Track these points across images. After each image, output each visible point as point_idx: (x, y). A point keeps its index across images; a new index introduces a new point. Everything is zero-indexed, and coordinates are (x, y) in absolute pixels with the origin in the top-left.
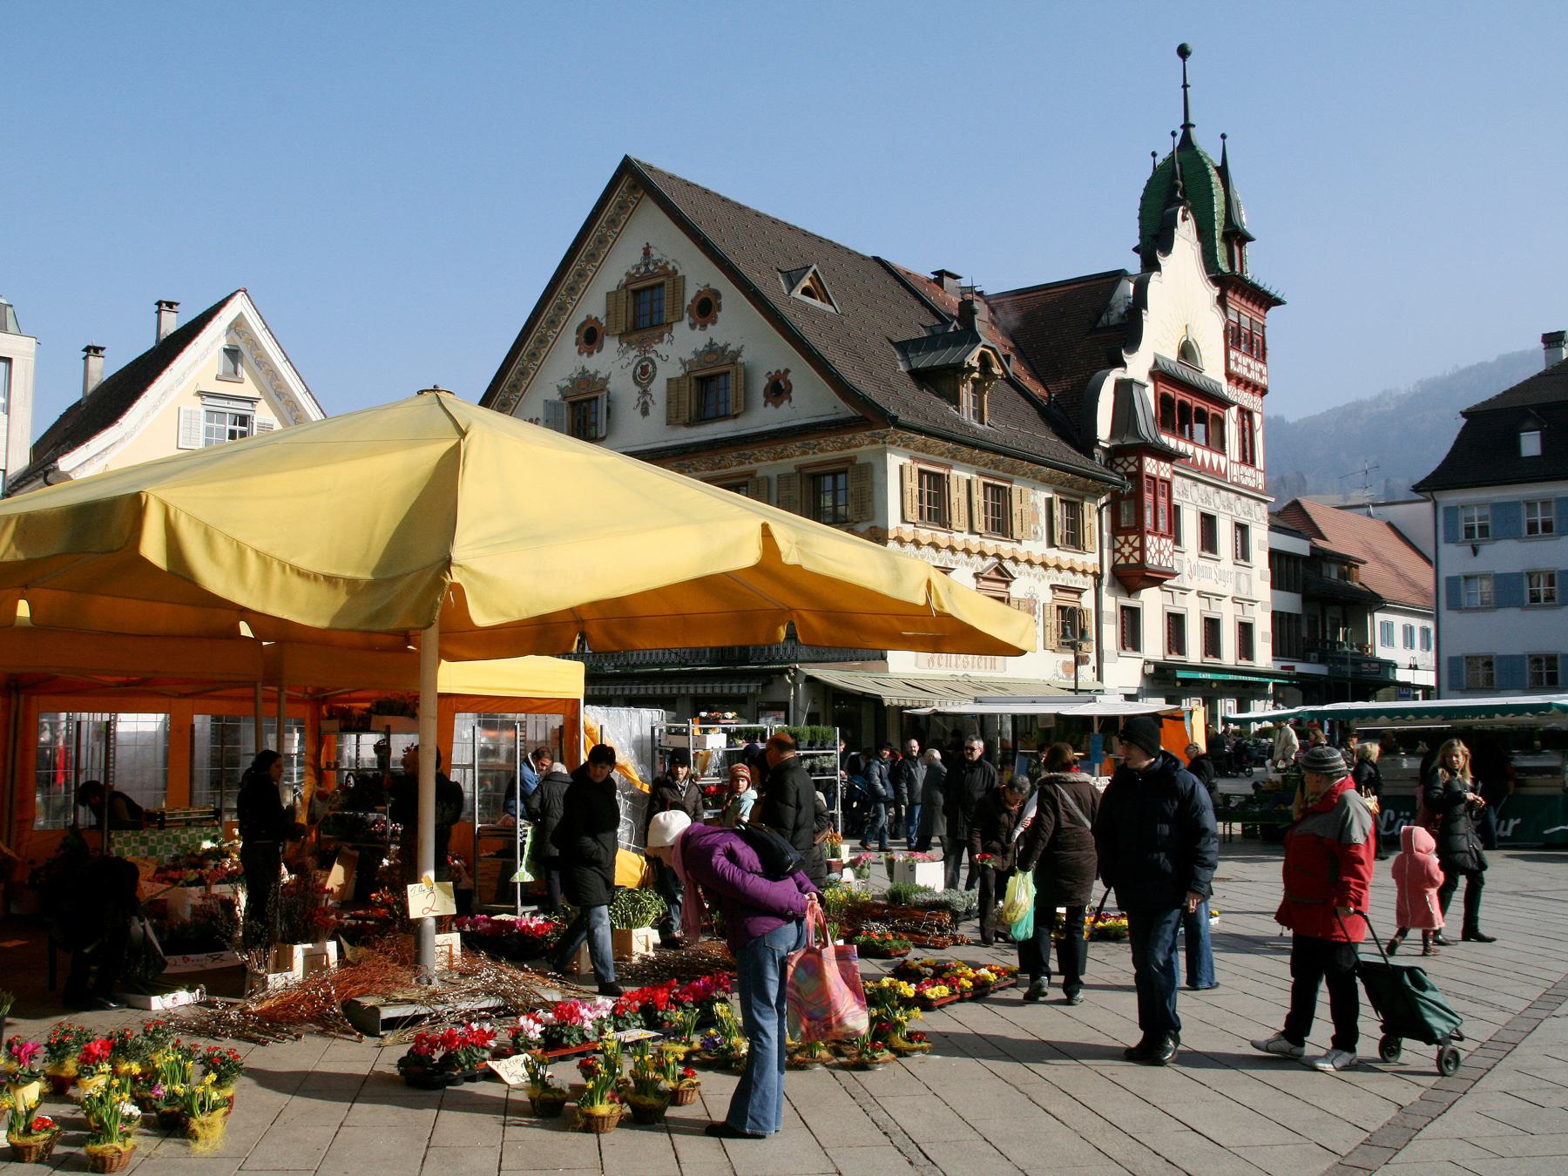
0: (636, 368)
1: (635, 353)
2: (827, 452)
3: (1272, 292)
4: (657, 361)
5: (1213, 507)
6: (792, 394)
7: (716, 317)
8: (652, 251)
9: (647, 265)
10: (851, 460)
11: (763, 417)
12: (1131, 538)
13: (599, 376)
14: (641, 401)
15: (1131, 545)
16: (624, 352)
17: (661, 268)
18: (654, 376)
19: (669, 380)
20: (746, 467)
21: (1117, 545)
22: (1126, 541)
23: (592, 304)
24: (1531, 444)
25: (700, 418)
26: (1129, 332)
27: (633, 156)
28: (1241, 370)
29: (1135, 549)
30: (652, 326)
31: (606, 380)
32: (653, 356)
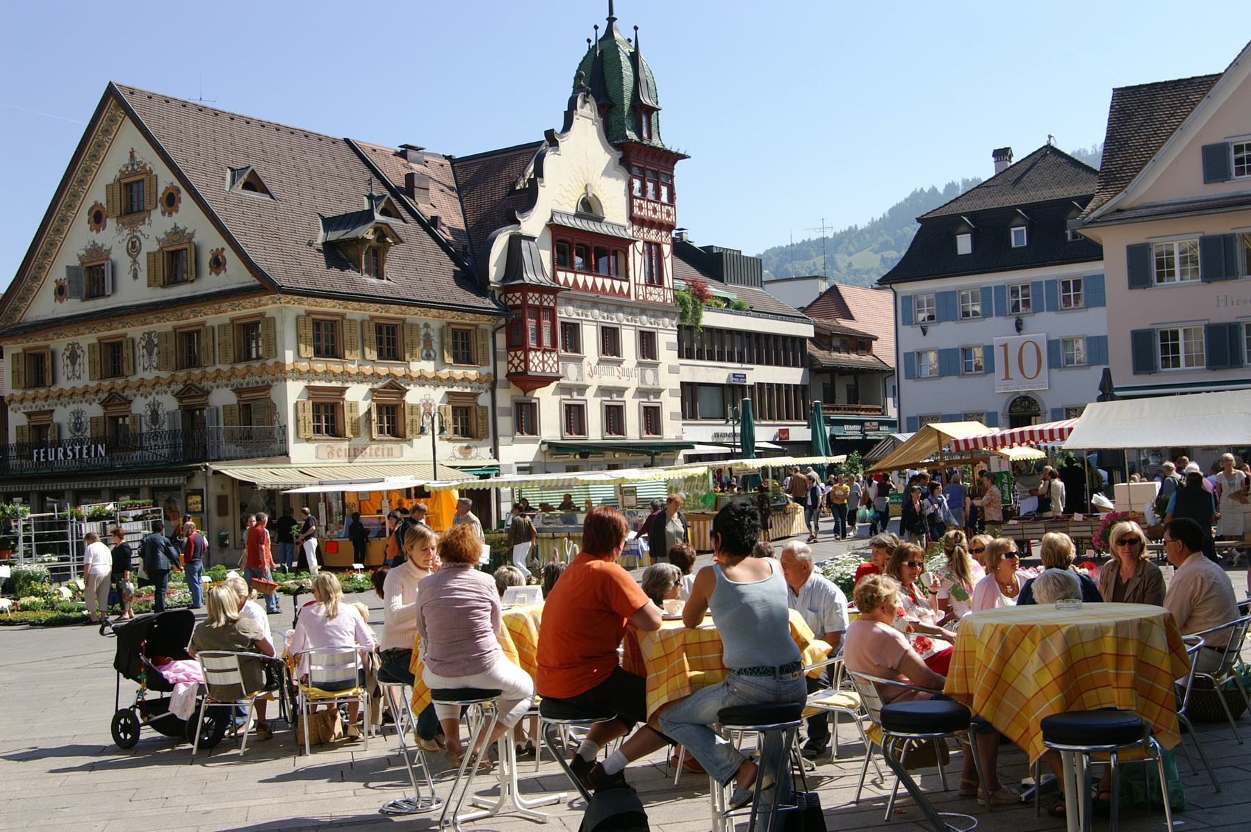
0: (128, 243)
2: (246, 309)
3: (674, 150)
4: (142, 238)
5: (615, 321)
7: (178, 207)
8: (136, 155)
9: (133, 165)
10: (262, 315)
11: (209, 283)
12: (519, 353)
13: (104, 248)
15: (518, 358)
16: (120, 231)
17: (142, 168)
19: (148, 253)
20: (199, 319)
21: (510, 359)
22: (516, 355)
23: (97, 194)
24: (964, 244)
25: (173, 279)
26: (528, 199)
27: (115, 81)
28: (644, 213)
29: (521, 361)
30: (139, 211)
31: (109, 252)
32: (139, 234)
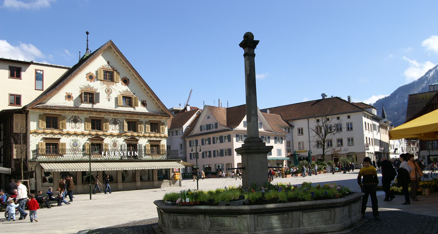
0: (106, 90)
1: (106, 85)
4: (112, 89)
6: (147, 106)
7: (128, 84)
13: (94, 88)
14: (108, 97)
18: (112, 93)
